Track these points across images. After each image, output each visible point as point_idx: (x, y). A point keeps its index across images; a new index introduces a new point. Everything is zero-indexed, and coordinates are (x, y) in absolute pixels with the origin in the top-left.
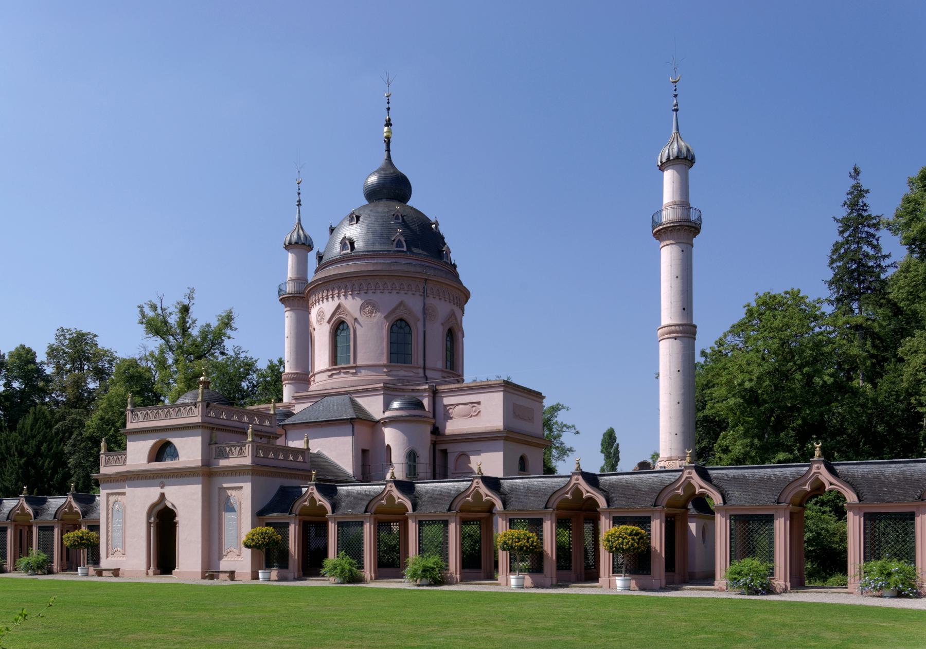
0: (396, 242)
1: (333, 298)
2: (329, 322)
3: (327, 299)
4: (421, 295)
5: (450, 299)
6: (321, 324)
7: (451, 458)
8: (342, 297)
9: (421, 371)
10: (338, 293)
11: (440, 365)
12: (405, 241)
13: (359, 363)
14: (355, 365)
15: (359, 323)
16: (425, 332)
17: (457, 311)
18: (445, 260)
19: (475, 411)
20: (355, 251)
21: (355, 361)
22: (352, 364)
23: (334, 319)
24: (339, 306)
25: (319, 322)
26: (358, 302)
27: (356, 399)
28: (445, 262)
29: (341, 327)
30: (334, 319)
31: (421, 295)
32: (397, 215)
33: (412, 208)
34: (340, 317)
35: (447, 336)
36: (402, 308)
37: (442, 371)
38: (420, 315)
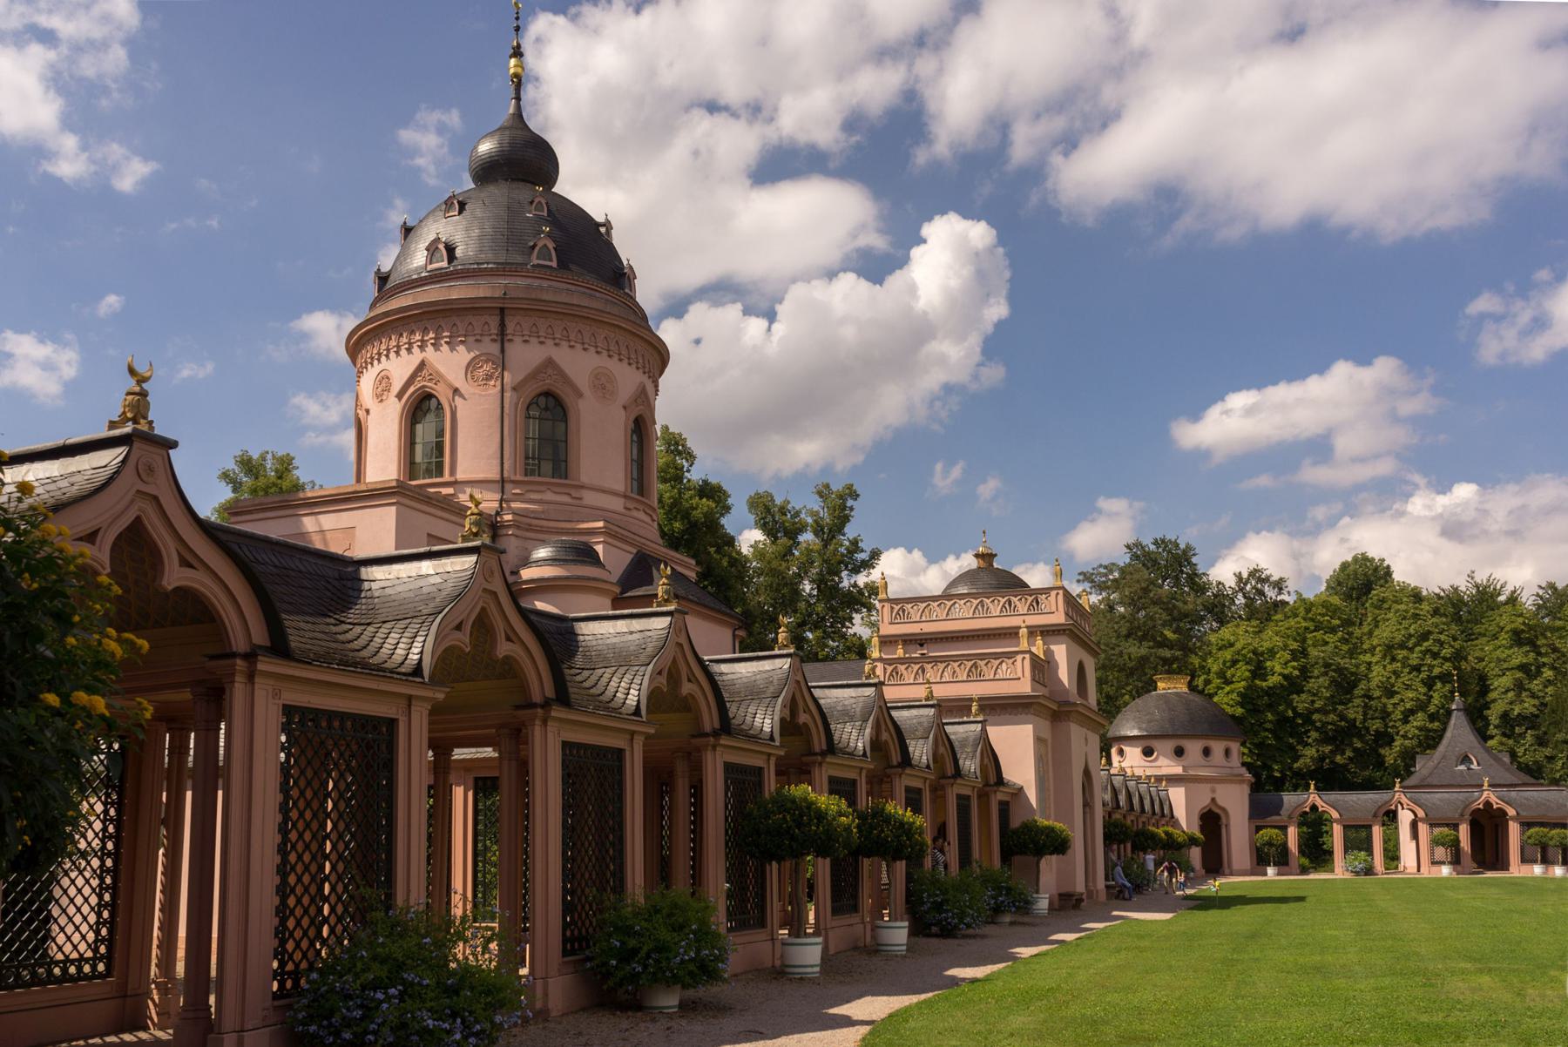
0: (537, 249)
1: (409, 350)
2: (399, 396)
3: (397, 353)
5: (637, 363)
6: (381, 401)
8: (430, 349)
10: (422, 341)
12: (555, 249)
13: (460, 476)
14: (452, 479)
15: (462, 396)
20: (455, 262)
21: (453, 472)
22: (447, 477)
23: (412, 389)
25: (380, 397)
26: (463, 355)
29: (425, 406)
30: (412, 389)
32: (540, 202)
33: (556, 194)
34: (424, 386)
35: (633, 432)
36: (550, 371)
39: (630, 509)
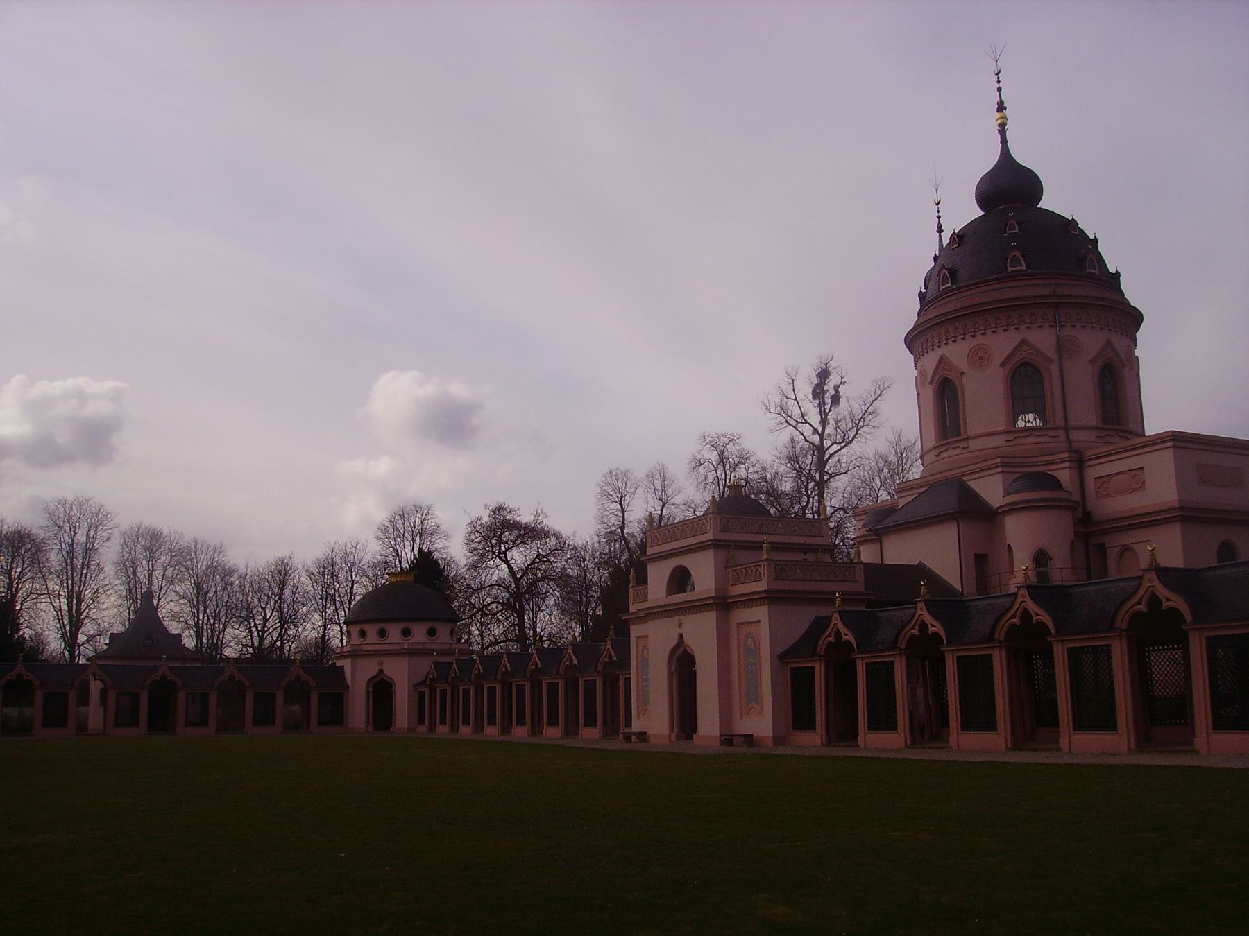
2: (931, 383)
4: (1051, 326)
7: (1112, 555)
9: (1061, 433)
10: (939, 342)
11: (1092, 420)
12: (1023, 256)
16: (1062, 376)
17: (1119, 342)
18: (1088, 270)
19: (1138, 483)
24: (941, 359)
27: (969, 483)
28: (1091, 273)
31: (1051, 326)
32: (1012, 224)
34: (943, 374)
37: (1097, 428)
38: (1052, 354)
39: (1102, 437)
